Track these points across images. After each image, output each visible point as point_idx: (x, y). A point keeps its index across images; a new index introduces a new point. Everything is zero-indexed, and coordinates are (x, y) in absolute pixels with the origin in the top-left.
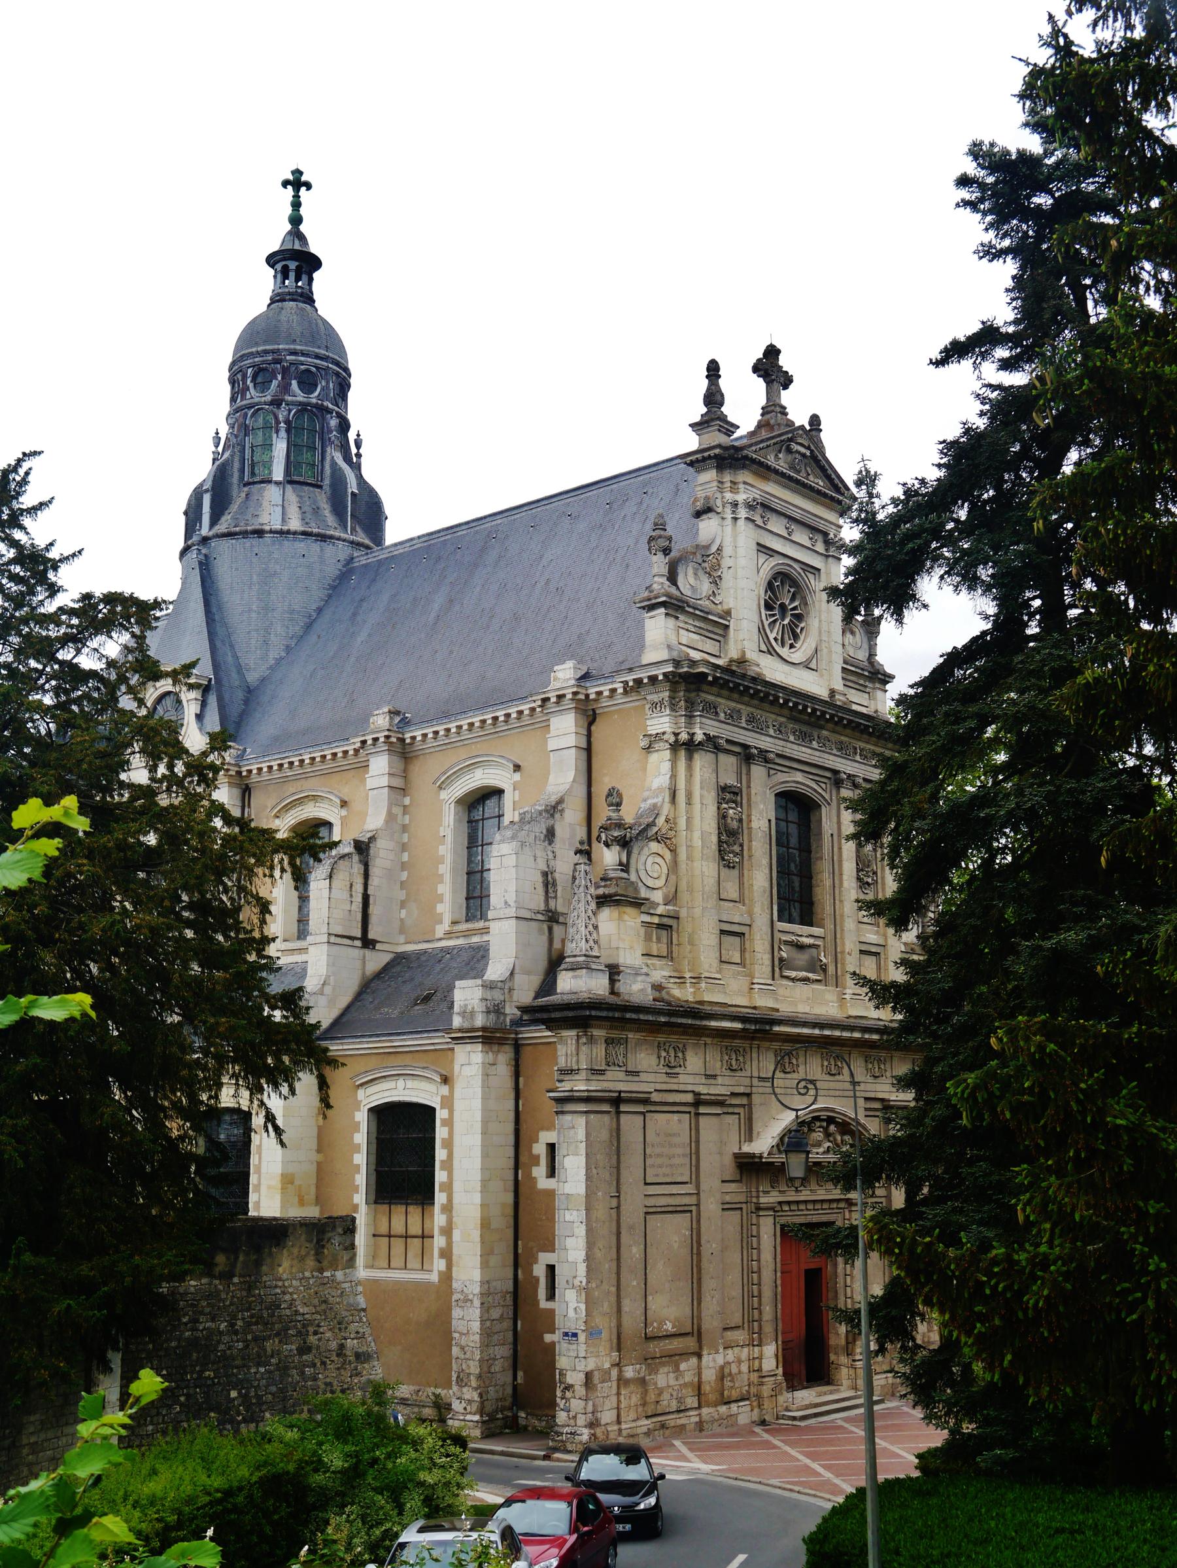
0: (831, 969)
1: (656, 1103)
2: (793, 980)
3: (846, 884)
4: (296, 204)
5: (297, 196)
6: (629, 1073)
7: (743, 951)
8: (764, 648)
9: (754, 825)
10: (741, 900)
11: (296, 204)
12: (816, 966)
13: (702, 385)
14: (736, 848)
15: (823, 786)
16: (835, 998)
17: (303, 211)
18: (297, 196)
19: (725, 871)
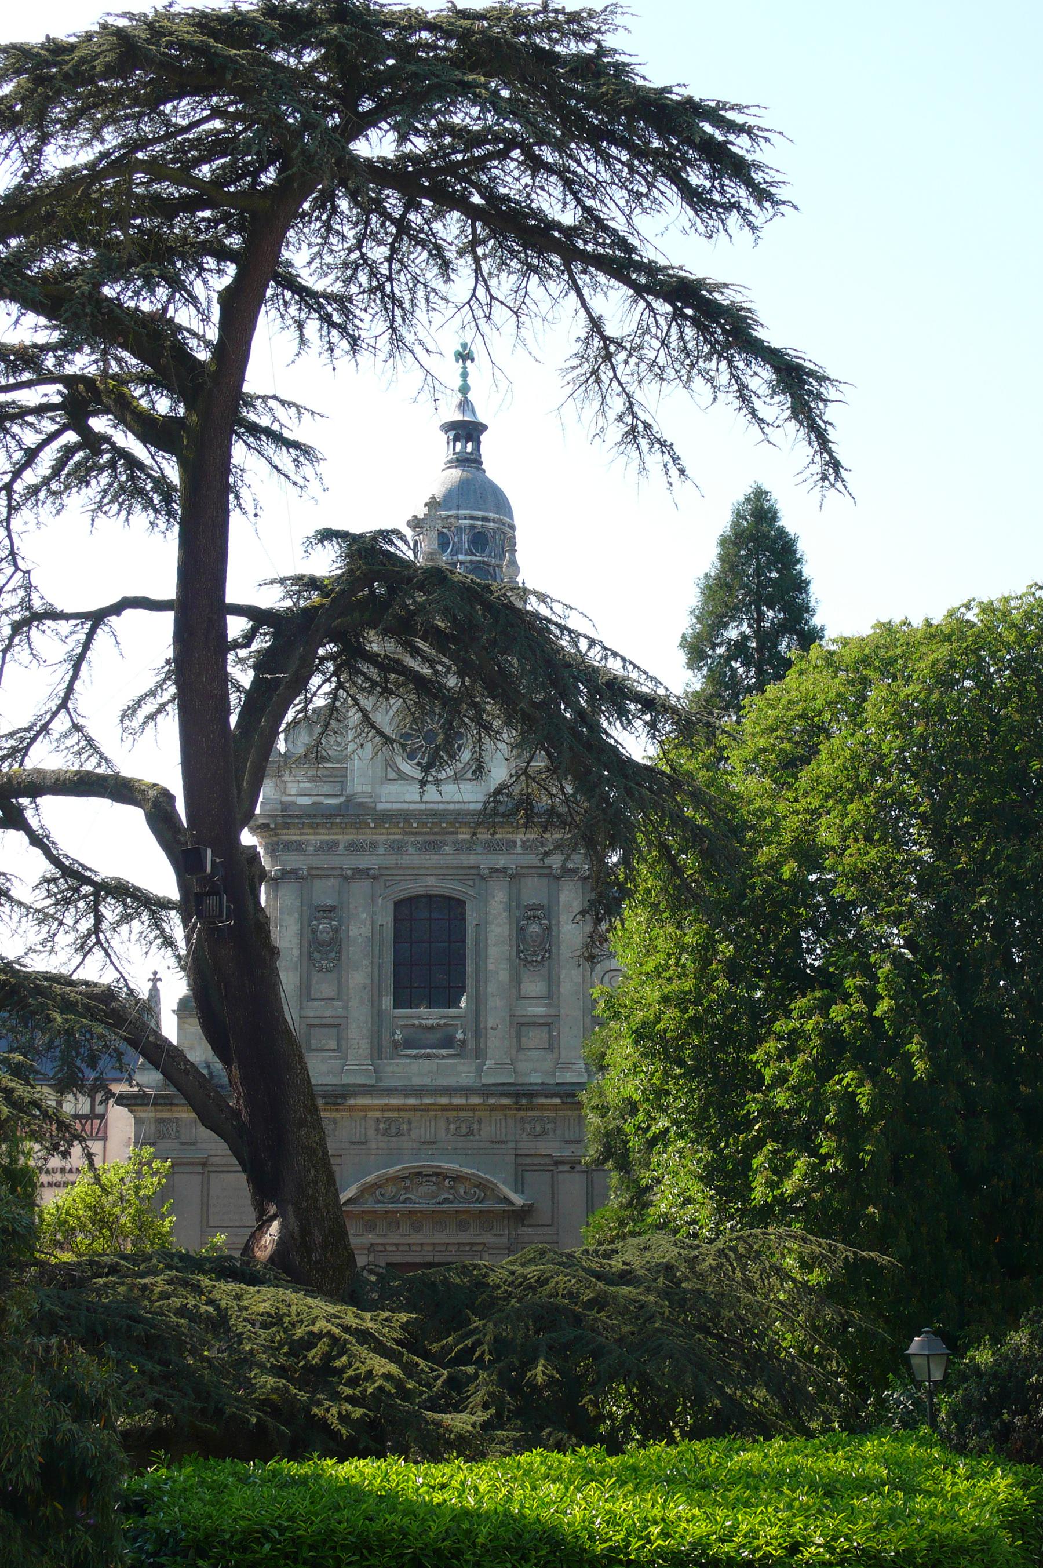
0: (471, 1044)
1: (218, 1165)
2: (415, 1057)
3: (491, 967)
4: (465, 375)
5: (465, 368)
6: (182, 1143)
7: (338, 1041)
8: (392, 775)
9: (354, 932)
10: (338, 998)
11: (465, 375)
12: (448, 1042)
13: (684, 462)
14: (333, 955)
15: (470, 883)
16: (473, 1069)
17: (469, 380)
18: (465, 368)
19: (316, 977)
